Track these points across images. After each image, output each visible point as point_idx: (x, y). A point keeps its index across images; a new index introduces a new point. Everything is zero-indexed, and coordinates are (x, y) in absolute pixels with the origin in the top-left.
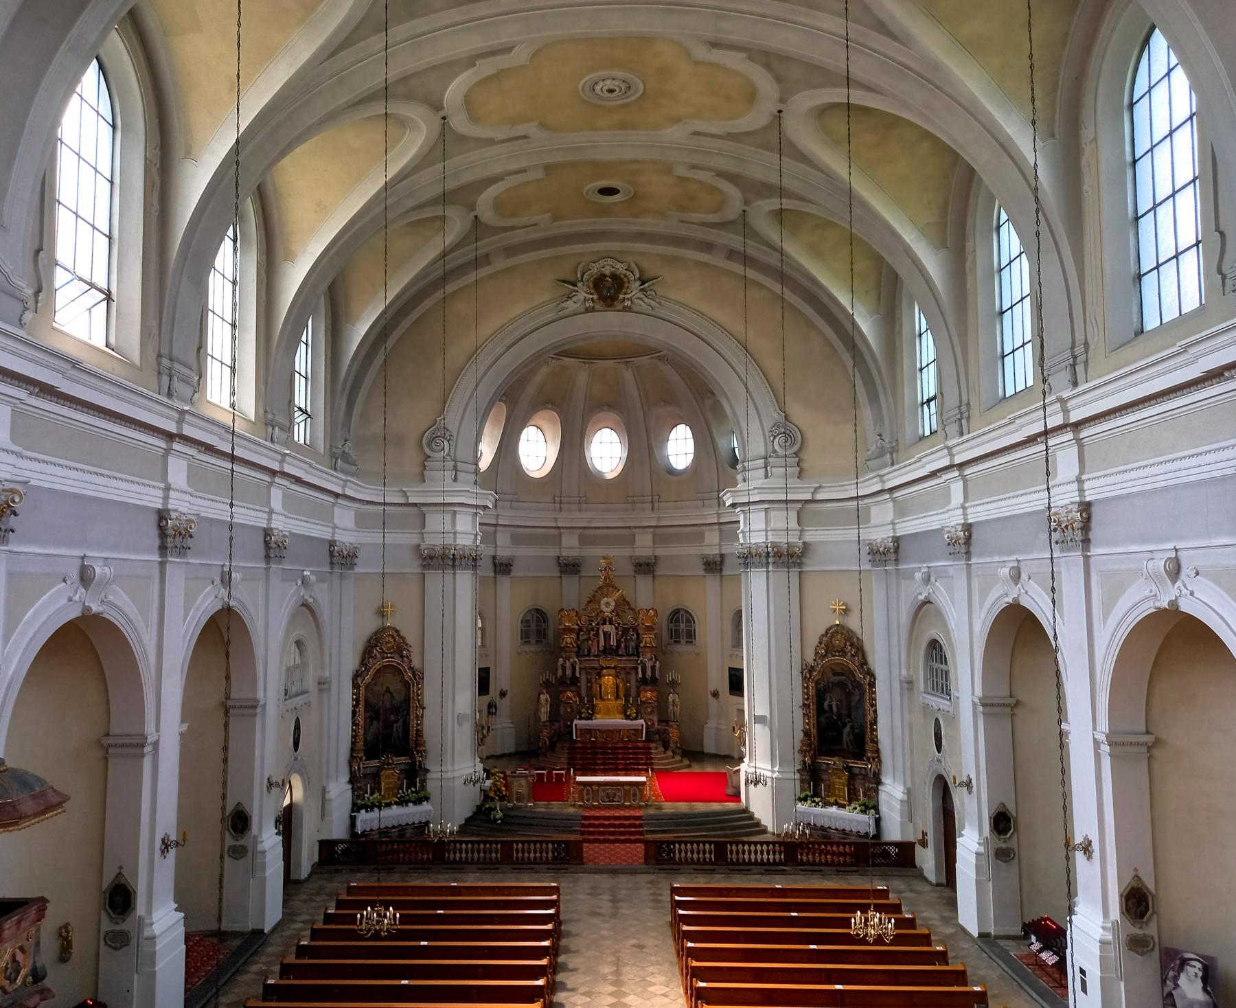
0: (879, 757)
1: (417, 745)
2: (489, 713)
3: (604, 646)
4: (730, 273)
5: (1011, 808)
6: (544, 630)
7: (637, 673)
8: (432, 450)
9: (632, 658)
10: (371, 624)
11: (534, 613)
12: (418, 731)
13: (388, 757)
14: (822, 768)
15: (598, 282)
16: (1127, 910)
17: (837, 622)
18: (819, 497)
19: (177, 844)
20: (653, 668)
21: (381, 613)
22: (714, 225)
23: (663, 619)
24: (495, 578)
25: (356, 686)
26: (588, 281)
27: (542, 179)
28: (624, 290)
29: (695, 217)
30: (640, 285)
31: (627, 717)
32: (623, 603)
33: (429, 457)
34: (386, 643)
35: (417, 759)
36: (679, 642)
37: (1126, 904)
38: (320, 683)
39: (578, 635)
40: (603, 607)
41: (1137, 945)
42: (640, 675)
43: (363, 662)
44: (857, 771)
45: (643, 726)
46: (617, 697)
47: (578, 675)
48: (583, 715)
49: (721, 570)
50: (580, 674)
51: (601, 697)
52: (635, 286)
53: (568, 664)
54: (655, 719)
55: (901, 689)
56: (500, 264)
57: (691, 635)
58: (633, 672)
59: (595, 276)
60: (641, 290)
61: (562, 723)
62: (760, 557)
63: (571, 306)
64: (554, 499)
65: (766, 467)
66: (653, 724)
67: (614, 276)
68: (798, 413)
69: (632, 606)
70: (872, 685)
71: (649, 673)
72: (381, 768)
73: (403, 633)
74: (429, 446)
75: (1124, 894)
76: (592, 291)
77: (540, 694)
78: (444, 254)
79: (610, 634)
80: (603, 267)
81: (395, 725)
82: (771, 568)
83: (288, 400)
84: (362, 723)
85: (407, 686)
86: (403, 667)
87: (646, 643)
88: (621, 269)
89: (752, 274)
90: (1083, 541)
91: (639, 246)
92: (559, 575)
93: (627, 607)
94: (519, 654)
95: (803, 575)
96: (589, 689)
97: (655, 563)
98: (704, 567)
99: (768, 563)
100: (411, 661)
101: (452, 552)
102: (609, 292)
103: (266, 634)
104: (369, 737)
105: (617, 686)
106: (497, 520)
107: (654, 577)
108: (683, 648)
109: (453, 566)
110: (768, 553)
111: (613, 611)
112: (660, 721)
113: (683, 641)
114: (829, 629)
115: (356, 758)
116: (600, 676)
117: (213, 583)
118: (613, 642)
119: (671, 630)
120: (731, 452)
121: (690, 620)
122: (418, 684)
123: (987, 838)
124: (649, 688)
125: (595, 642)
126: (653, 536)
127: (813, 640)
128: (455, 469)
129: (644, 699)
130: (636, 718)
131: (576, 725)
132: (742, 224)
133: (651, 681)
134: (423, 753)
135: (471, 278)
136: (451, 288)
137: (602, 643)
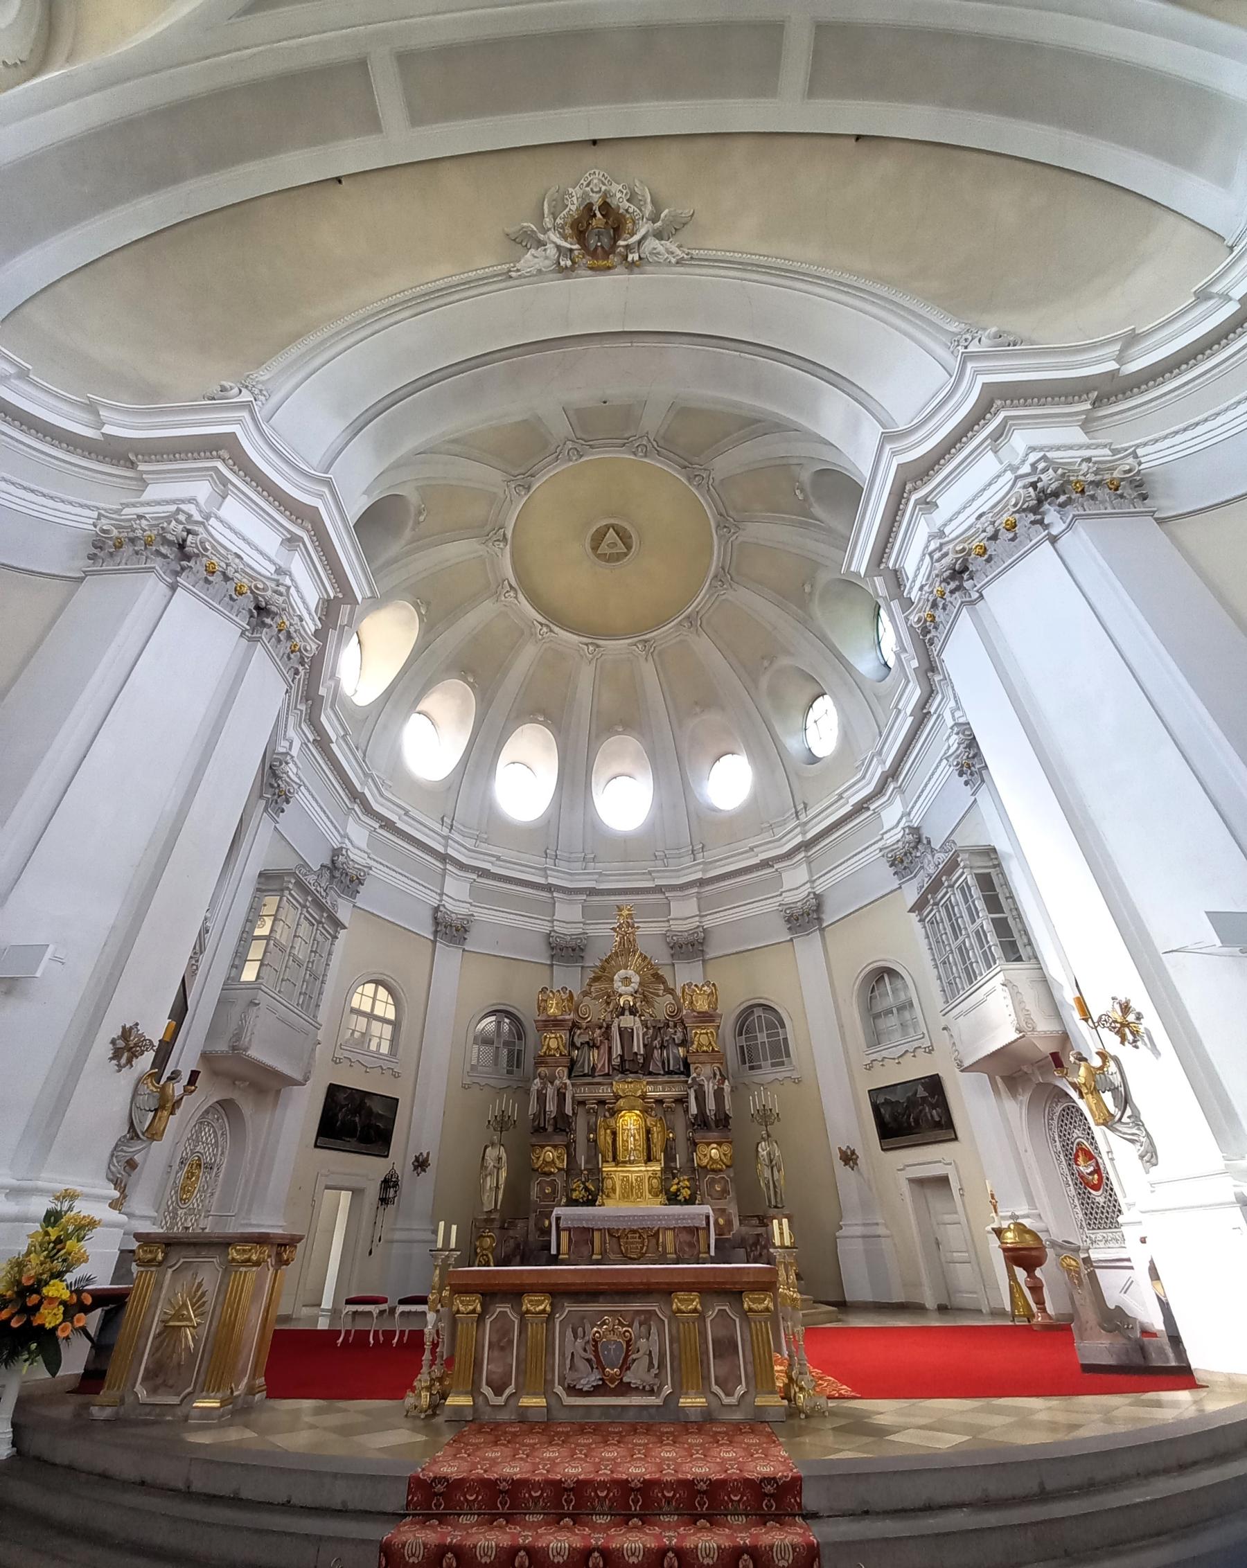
3: (622, 1056)
6: (519, 1051)
7: (687, 1111)
9: (675, 1078)
20: (719, 1094)
23: (729, 1009)
24: (434, 942)
31: (673, 1199)
36: (760, 1067)
39: (572, 1036)
40: (618, 985)
42: (694, 1109)
45: (708, 1218)
47: (568, 1110)
48: (575, 1195)
49: (819, 920)
50: (573, 1110)
51: (614, 1159)
53: (550, 1091)
54: (733, 1210)
57: (780, 1051)
58: (680, 1109)
61: (532, 1222)
66: (729, 1223)
71: (711, 1105)
77: (486, 1147)
79: (633, 1029)
87: (700, 1045)
96: (593, 1145)
105: (648, 1132)
107: (704, 961)
108: (767, 1073)
112: (743, 1219)
116: (614, 1113)
118: (638, 1046)
119: (742, 1047)
120: (807, 753)
121: (776, 1021)
124: (714, 1135)
125: (604, 1049)
126: (699, 899)
129: (705, 1162)
130: (690, 1201)
131: (558, 1219)
133: (717, 1123)
137: (617, 1050)
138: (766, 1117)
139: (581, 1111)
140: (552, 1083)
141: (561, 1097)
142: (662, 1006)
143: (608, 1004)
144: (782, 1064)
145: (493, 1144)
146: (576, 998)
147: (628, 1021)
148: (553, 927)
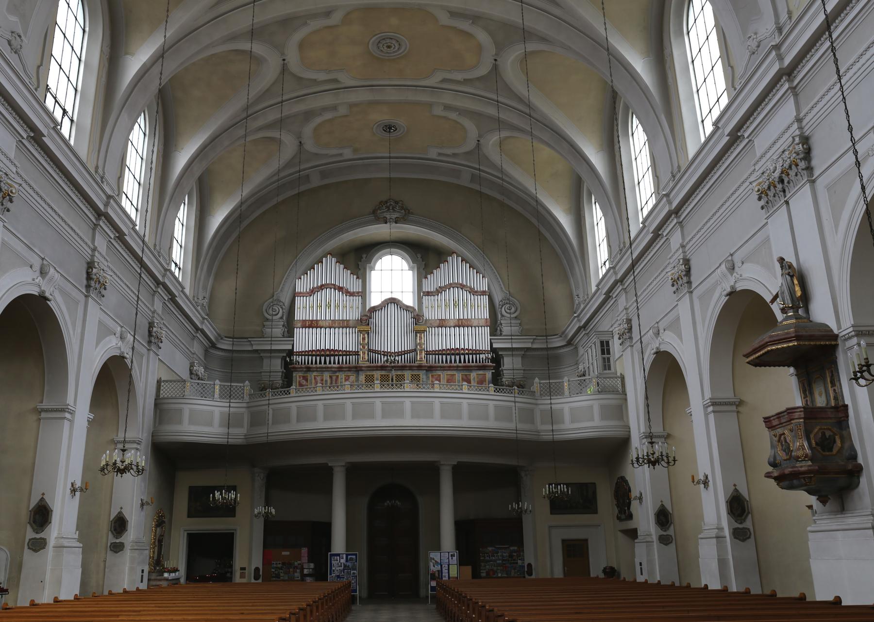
19: (81, 490)
27: (346, 116)
83: (169, 247)
90: (687, 283)
117: (115, 335)
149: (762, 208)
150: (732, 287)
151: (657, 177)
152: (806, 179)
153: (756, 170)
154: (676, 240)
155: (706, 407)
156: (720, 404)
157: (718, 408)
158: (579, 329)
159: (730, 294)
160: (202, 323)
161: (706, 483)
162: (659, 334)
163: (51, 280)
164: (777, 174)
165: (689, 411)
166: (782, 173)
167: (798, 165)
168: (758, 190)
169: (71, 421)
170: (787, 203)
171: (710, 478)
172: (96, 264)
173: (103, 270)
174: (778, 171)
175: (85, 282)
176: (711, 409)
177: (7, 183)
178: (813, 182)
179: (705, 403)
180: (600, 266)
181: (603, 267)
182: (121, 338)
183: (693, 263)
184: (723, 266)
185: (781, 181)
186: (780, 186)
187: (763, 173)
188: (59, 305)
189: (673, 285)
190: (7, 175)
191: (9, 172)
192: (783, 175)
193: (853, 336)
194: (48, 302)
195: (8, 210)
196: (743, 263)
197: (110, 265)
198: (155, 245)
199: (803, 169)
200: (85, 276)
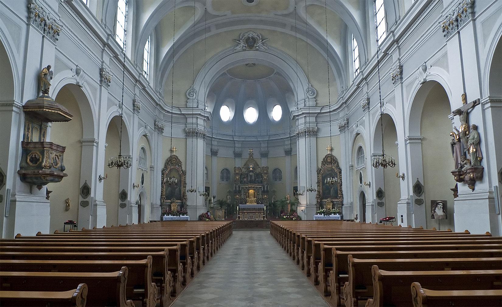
0: (343, 196)
1: (183, 196)
2: (209, 203)
3: (250, 180)
4: (291, 36)
5: (383, 189)
8: (190, 96)
10: (168, 155)
11: (225, 170)
12: (184, 192)
13: (174, 199)
14: (324, 203)
15: (247, 40)
16: (415, 191)
17: (329, 153)
18: (322, 112)
20: (267, 187)
21: (171, 151)
22: (285, 15)
23: (270, 171)
24: (212, 156)
25: (163, 174)
26: (244, 40)
28: (256, 43)
29: (279, 13)
30: (262, 41)
32: (256, 165)
33: (189, 99)
34: (173, 161)
35: (184, 201)
37: (415, 189)
38: (151, 167)
41: (419, 202)
42: (263, 190)
43: (166, 166)
44: (335, 203)
46: (254, 198)
50: (241, 189)
52: (260, 43)
53: (237, 186)
55: (350, 170)
56: (214, 31)
57: (280, 179)
59: (246, 38)
60: (262, 43)
62: (303, 133)
63: (239, 48)
64: (233, 131)
65: (305, 103)
67: (253, 38)
68: (317, 86)
69: (260, 166)
70: (340, 173)
72: (171, 203)
73: (179, 158)
74: (189, 95)
75: (414, 186)
76: (245, 43)
77: (227, 196)
78: (194, 25)
80: (249, 35)
81: (176, 189)
82: (306, 136)
84: (165, 187)
85: (180, 176)
86: (179, 169)
87: (265, 178)
88: (255, 35)
89: (299, 36)
91: (262, 27)
92: (234, 157)
93: (258, 167)
94: (220, 184)
95: (317, 139)
97: (268, 153)
98: (285, 153)
99: (306, 135)
100: (182, 168)
101: (196, 131)
102: (251, 44)
103: (133, 135)
104: (167, 192)
105: (254, 193)
106: (212, 135)
109: (197, 136)
110: (306, 131)
111: (253, 168)
113: (278, 180)
114: (326, 156)
115: (163, 197)
116: (249, 190)
118: (253, 178)
122: (184, 176)
123: (375, 199)
127: (321, 160)
128: (198, 102)
132: (295, 14)
134: (186, 199)
135: (203, 37)
136: (197, 40)
138: (274, 192)
139: (242, 189)
140: (237, 185)
141: (239, 187)
142: (258, 171)
143: (248, 170)
144: (280, 180)
145: (228, 195)
146: (241, 168)
147: (251, 174)
148: (235, 149)
149: (445, 36)
150: (424, 79)
151: (388, 23)
152: (471, 19)
153: (443, 16)
154: (395, 56)
155: (406, 141)
156: (413, 139)
157: (412, 141)
158: (343, 103)
159: (423, 83)
160: (159, 101)
161: (403, 178)
162: (383, 105)
163: (82, 77)
164: (454, 17)
165: (397, 143)
166: (458, 16)
167: (467, 11)
168: (443, 26)
169: (97, 147)
170: (459, 32)
171: (406, 175)
172: (104, 69)
173: (108, 72)
174: (456, 15)
175: (99, 79)
176: (408, 141)
177: (55, 25)
178: (474, 20)
179: (405, 139)
180: (354, 72)
181: (356, 72)
182: (119, 107)
183: (404, 68)
184: (421, 68)
185: (457, 20)
186: (455, 24)
187: (447, 17)
188: (87, 90)
189: (393, 80)
190: (55, 21)
191: (56, 20)
192: (458, 17)
193: (488, 102)
194: (81, 88)
195: (57, 40)
196: (431, 67)
197: (112, 70)
198: (134, 61)
199: (469, 13)
200: (99, 75)
